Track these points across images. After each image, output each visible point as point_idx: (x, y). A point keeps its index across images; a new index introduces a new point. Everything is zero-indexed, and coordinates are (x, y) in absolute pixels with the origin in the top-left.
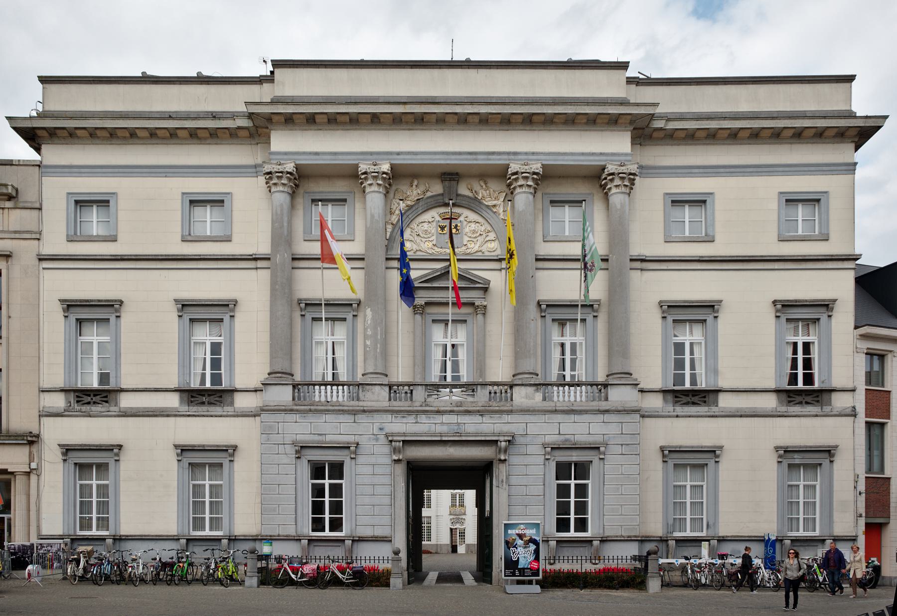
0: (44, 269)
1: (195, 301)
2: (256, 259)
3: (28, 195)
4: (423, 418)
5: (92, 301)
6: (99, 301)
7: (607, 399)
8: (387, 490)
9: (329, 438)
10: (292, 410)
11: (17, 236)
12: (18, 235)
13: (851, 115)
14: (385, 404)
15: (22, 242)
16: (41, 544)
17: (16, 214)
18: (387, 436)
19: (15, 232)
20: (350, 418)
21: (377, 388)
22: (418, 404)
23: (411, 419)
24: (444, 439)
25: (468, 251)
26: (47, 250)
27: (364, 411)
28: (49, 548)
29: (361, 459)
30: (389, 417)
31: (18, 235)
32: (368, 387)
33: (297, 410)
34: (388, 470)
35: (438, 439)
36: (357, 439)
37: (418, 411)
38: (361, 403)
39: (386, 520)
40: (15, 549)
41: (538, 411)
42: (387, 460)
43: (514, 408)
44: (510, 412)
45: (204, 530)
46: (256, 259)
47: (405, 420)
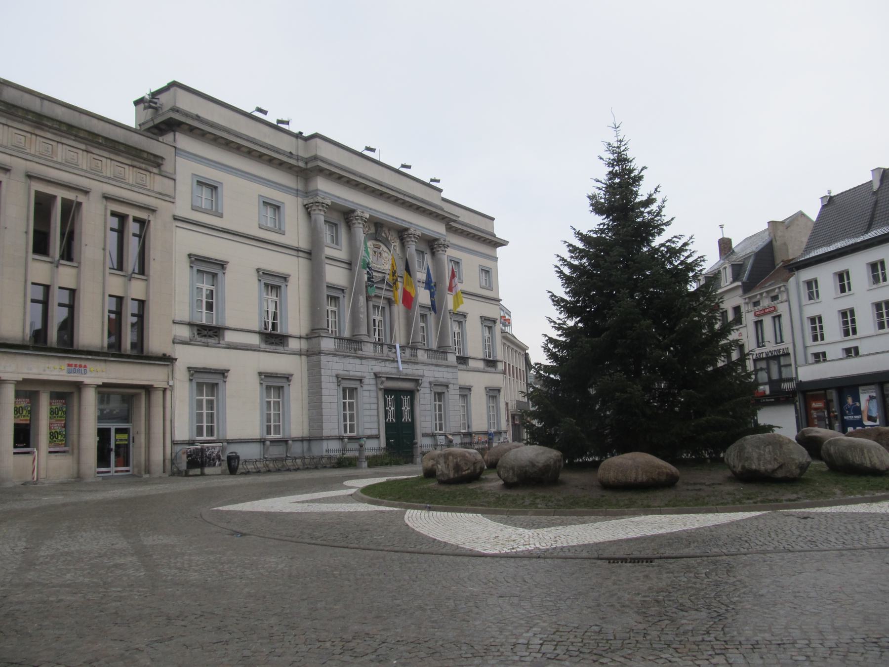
0: (177, 226)
1: (269, 271)
2: (298, 251)
3: (167, 167)
4: (387, 364)
5: (211, 259)
6: (216, 260)
7: (447, 360)
8: (374, 406)
9: (352, 373)
10: (335, 354)
11: (161, 197)
12: (162, 196)
13: (494, 236)
14: (372, 354)
15: (163, 202)
16: (208, 447)
17: (158, 178)
18: (375, 374)
19: (160, 194)
20: (358, 361)
21: (369, 344)
22: (385, 355)
23: (383, 364)
24: (401, 377)
25: (385, 268)
26: (180, 213)
27: (365, 358)
28: (213, 450)
29: (365, 387)
30: (374, 362)
31: (162, 196)
32: (365, 343)
33: (338, 355)
34: (374, 394)
35: (398, 377)
36: (363, 374)
37: (386, 360)
38: (364, 353)
39: (376, 425)
40: (190, 452)
41: (426, 364)
42: (374, 388)
43: (419, 361)
44: (417, 363)
45: (270, 435)
46: (298, 251)
47: (381, 365)
